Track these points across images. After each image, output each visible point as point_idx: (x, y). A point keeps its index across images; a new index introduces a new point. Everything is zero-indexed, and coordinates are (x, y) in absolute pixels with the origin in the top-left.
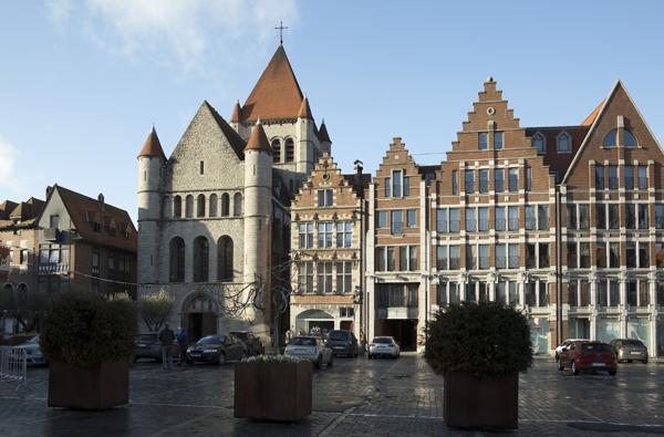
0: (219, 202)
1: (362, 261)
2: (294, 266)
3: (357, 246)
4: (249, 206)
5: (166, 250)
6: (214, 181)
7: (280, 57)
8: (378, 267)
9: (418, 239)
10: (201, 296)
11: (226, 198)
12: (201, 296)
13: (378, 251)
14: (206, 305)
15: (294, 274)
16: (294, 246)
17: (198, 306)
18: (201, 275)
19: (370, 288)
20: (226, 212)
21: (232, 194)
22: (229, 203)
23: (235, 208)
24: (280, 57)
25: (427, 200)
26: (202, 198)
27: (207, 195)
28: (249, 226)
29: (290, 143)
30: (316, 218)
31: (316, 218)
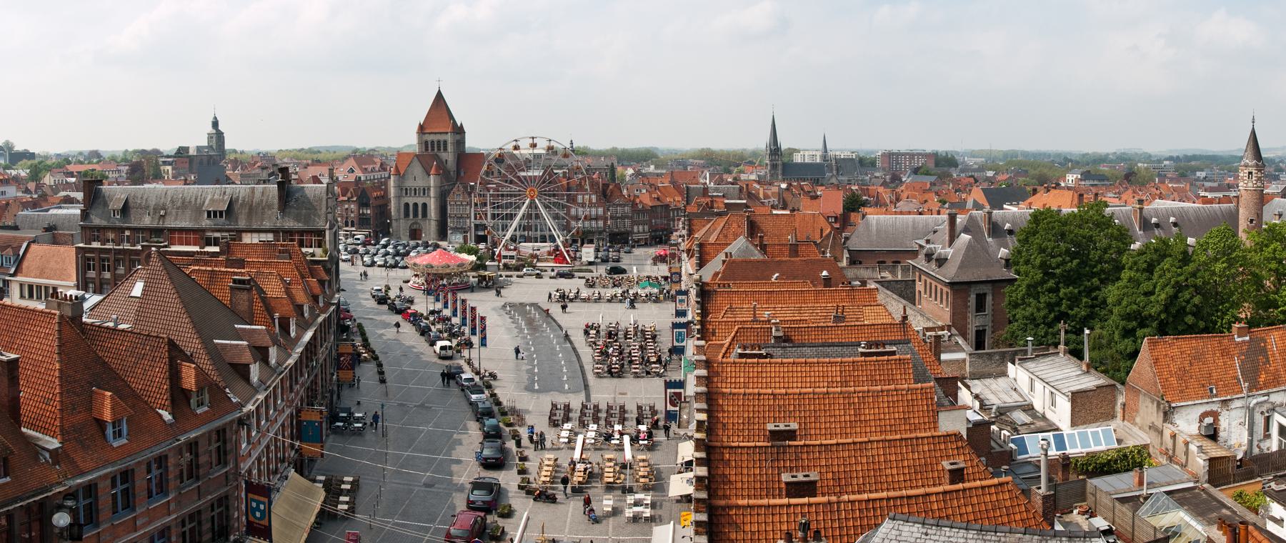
1: (470, 218)
4: (432, 194)
6: (420, 183)
7: (439, 97)
8: (476, 218)
10: (416, 223)
11: (424, 190)
12: (416, 223)
13: (475, 215)
15: (449, 220)
16: (449, 212)
17: (415, 227)
18: (416, 215)
19: (473, 225)
20: (424, 194)
22: (425, 191)
24: (439, 97)
26: (415, 189)
28: (432, 200)
29: (445, 142)
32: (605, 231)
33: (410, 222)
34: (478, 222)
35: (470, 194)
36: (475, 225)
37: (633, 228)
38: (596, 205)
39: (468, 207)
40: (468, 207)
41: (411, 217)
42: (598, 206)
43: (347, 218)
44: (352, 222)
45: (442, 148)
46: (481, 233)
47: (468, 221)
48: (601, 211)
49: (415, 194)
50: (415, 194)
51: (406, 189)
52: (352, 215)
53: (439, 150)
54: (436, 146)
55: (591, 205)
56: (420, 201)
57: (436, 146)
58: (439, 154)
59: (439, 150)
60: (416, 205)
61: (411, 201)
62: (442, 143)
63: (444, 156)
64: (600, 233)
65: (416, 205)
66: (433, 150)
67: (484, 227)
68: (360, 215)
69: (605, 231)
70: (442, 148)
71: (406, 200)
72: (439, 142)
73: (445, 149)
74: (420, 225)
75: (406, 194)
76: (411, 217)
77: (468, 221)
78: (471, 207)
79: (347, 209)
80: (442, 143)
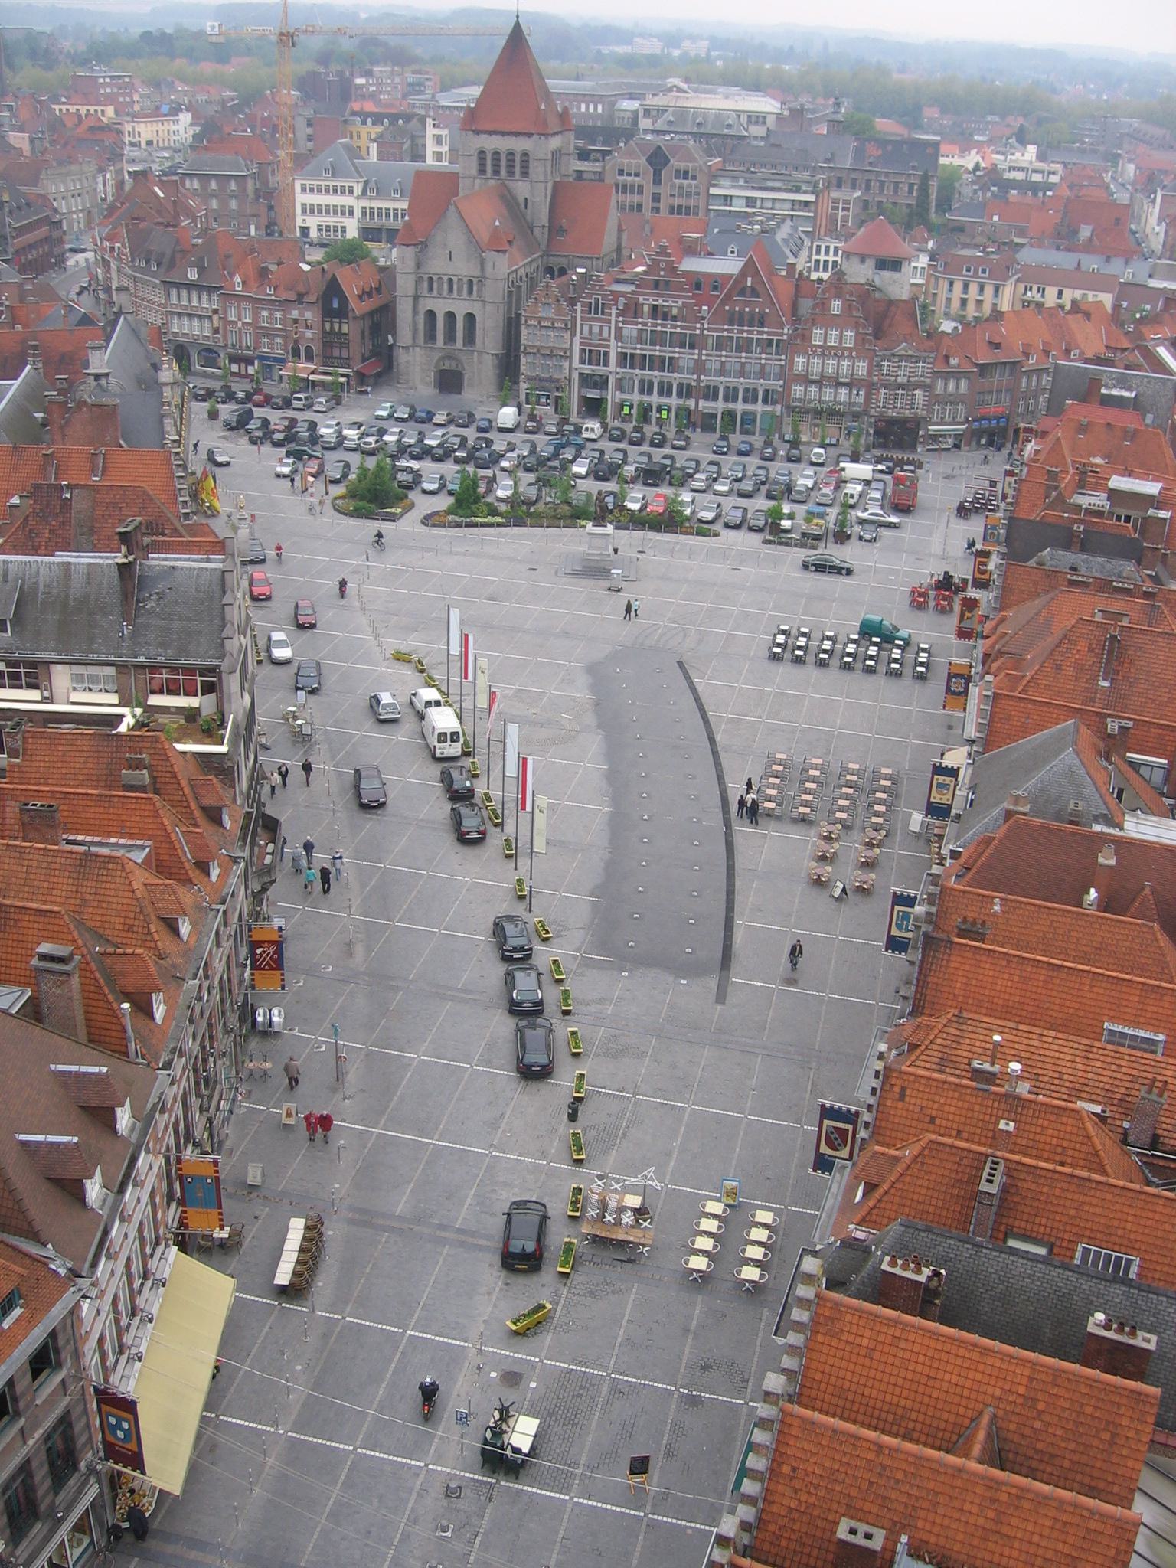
0: (465, 287)
1: (570, 358)
2: (522, 355)
3: (567, 346)
5: (421, 319)
8: (582, 362)
9: (608, 346)
11: (471, 282)
14: (454, 364)
15: (523, 360)
16: (523, 341)
17: (447, 365)
19: (575, 376)
20: (470, 292)
21: (475, 281)
23: (478, 291)
25: (617, 322)
27: (455, 279)
30: (539, 323)
31: (539, 323)
32: (865, 412)
33: (437, 355)
34: (587, 369)
35: (572, 303)
36: (581, 374)
37: (930, 411)
38: (852, 354)
39: (567, 335)
40: (567, 335)
41: (440, 341)
42: (859, 357)
43: (296, 342)
44: (308, 349)
45: (517, 169)
46: (593, 394)
47: (566, 364)
48: (862, 367)
49: (451, 290)
50: (451, 290)
51: (431, 279)
52: (309, 334)
53: (511, 173)
54: (503, 163)
55: (838, 353)
56: (461, 309)
57: (503, 163)
58: (511, 184)
59: (511, 173)
60: (450, 316)
61: (441, 307)
62: (518, 159)
63: (521, 189)
64: (856, 416)
65: (450, 316)
66: (496, 172)
67: (601, 383)
68: (324, 331)
69: (865, 412)
70: (517, 169)
71: (428, 304)
72: (511, 154)
73: (525, 173)
74: (457, 360)
75: (431, 289)
76: (440, 341)
77: (566, 364)
78: (573, 335)
79: (296, 321)
80: (518, 159)
